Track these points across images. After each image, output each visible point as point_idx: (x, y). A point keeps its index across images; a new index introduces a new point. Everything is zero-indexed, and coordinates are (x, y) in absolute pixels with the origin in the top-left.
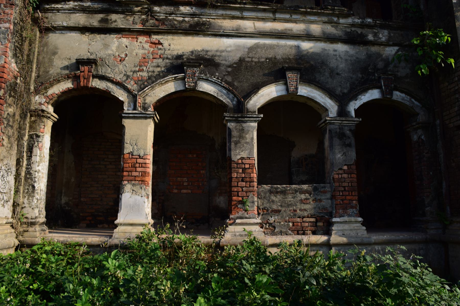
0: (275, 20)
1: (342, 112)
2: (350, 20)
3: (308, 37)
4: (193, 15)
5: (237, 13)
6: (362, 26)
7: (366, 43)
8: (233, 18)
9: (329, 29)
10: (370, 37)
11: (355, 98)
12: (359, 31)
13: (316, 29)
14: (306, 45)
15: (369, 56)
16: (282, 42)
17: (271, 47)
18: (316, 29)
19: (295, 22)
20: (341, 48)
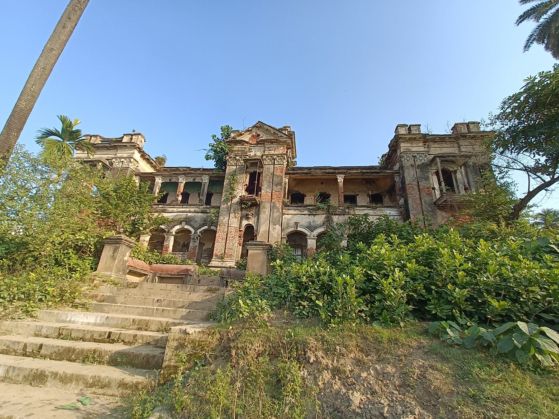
0: (183, 208)
1: (195, 233)
2: (203, 207)
3: (190, 212)
4: (162, 207)
5: (173, 207)
6: (206, 208)
7: (207, 213)
8: (172, 208)
9: (197, 209)
10: (208, 211)
11: (200, 228)
12: (205, 209)
13: (192, 210)
14: (189, 214)
15: (207, 216)
16: (184, 214)
17: (181, 215)
18: (192, 210)
19: (188, 208)
20: (200, 214)
